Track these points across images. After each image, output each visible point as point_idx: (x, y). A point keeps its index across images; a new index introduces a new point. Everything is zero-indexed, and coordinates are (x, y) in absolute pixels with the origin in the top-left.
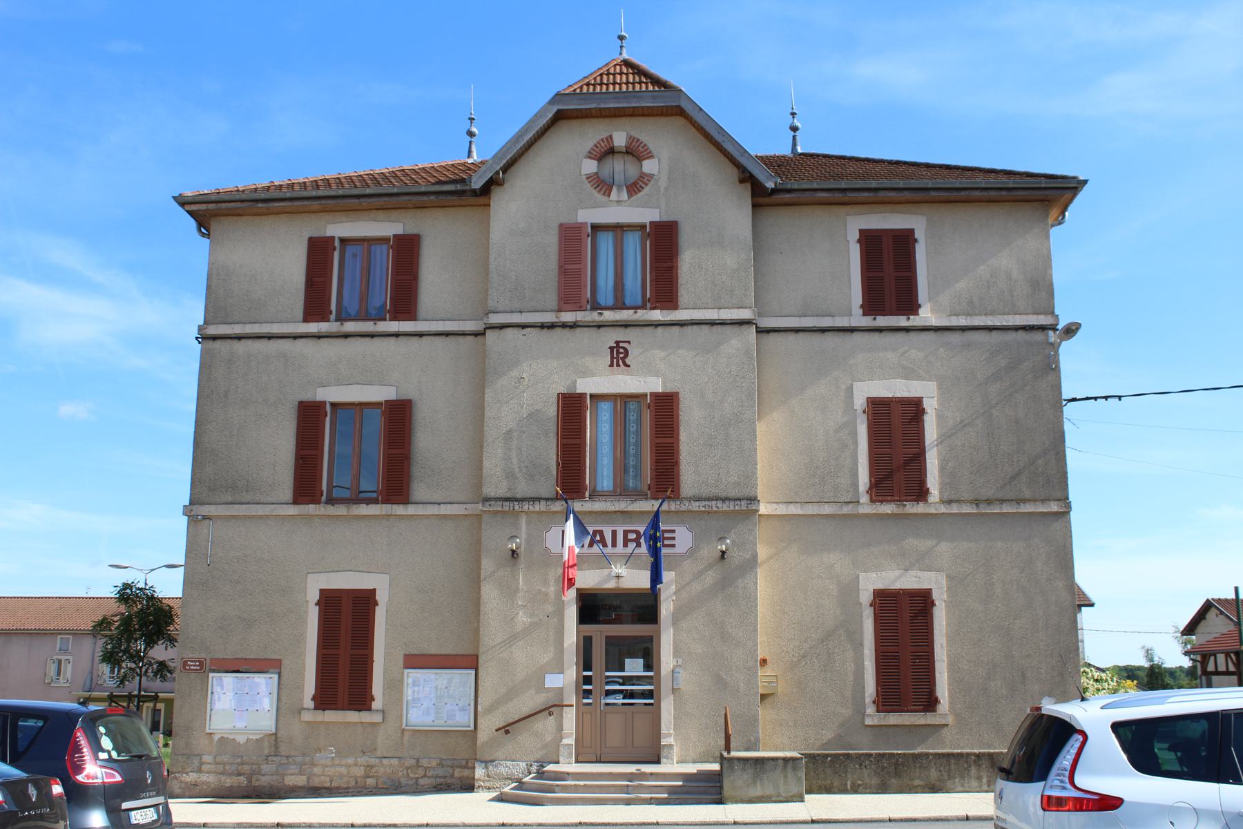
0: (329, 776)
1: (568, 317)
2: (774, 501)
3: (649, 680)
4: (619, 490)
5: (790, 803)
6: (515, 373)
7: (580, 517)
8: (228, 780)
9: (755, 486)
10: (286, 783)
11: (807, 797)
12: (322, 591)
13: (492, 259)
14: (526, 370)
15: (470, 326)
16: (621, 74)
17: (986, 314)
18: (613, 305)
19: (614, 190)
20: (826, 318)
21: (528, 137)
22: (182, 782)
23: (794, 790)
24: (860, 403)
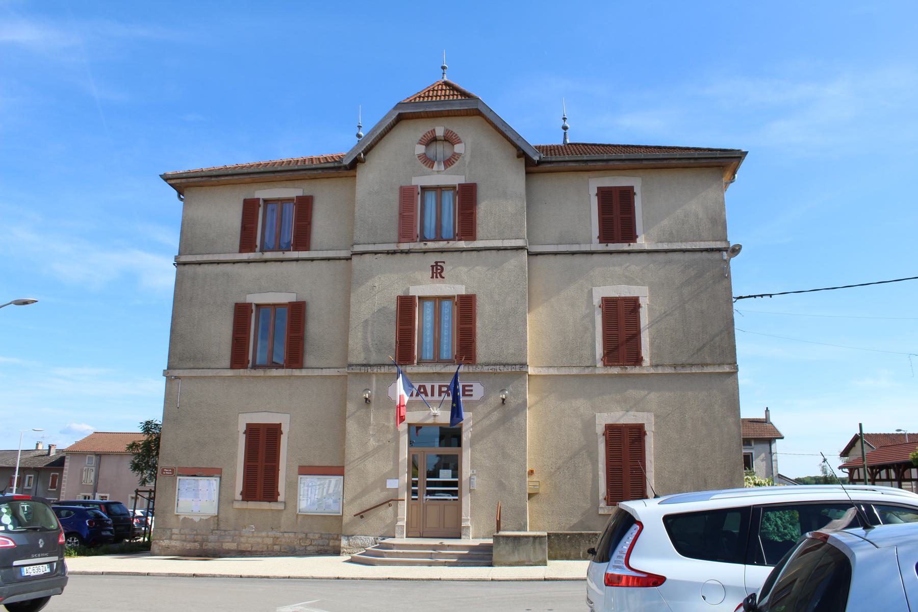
1: (405, 246)
5: (537, 567)
6: (370, 283)
7: (408, 376)
10: (224, 548)
11: (549, 562)
12: (248, 425)
13: (357, 209)
14: (378, 281)
15: (344, 254)
16: (442, 90)
17: (681, 242)
18: (435, 238)
19: (436, 164)
20: (575, 245)
21: (379, 132)
22: (160, 546)
23: (540, 558)
24: (597, 301)
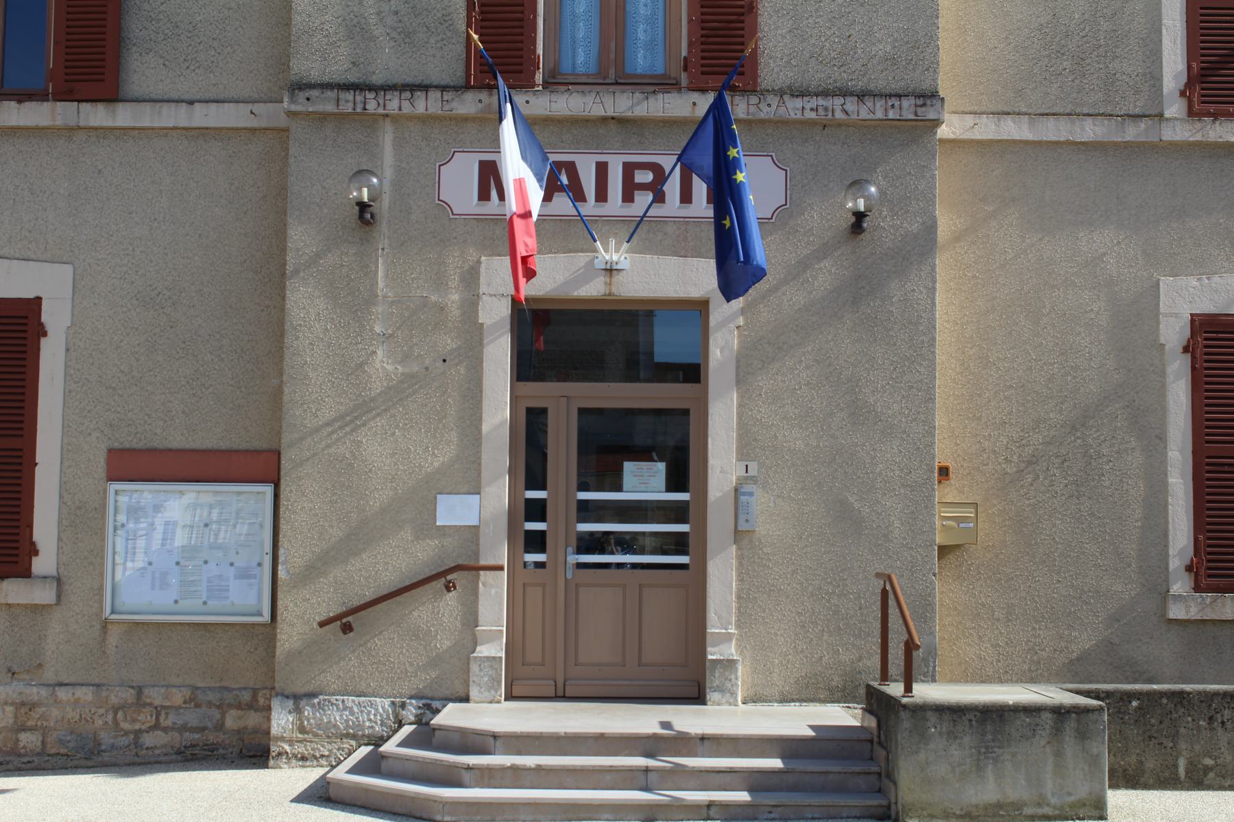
2: (969, 109)
3: (678, 513)
4: (612, 72)
9: (933, 67)
23: (1082, 791)
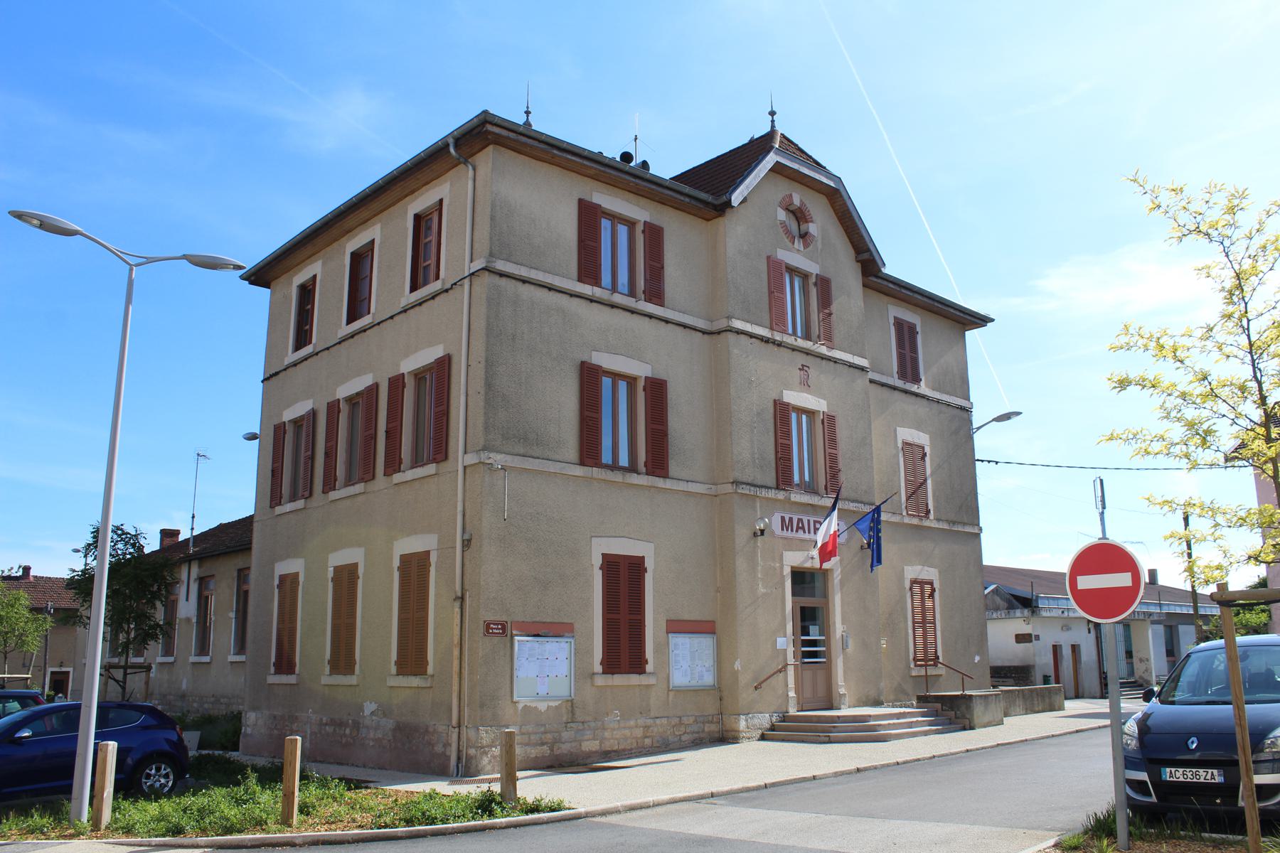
0: (617, 739)
8: (533, 751)
10: (583, 749)
15: (701, 324)
